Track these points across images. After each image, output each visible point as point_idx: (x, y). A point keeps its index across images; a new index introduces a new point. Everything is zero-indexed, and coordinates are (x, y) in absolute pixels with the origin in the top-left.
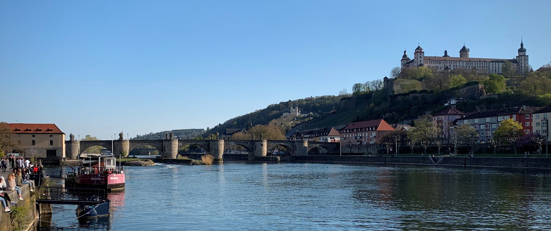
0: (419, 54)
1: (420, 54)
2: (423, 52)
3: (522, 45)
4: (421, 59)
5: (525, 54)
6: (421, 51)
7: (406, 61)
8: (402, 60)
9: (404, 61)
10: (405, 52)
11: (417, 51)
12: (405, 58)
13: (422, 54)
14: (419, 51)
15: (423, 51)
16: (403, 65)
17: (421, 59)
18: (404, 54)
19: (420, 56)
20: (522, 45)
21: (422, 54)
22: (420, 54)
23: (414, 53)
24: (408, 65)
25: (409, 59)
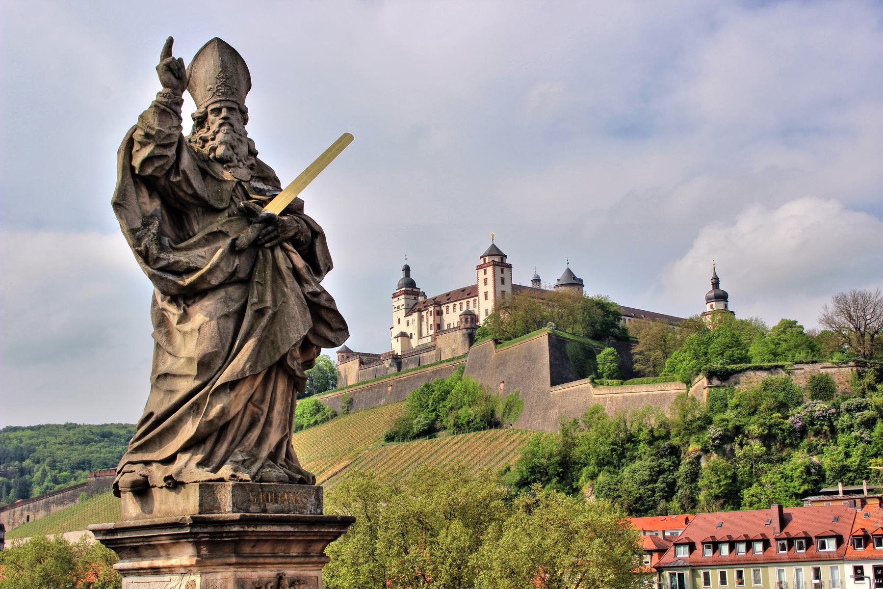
1: (502, 272)
2: (509, 266)
3: (716, 283)
4: (503, 288)
5: (726, 306)
6: (502, 259)
7: (413, 297)
9: (408, 296)
10: (407, 269)
12: (410, 289)
13: (505, 270)
14: (497, 259)
15: (508, 261)
17: (503, 288)
19: (503, 276)
20: (716, 283)
21: (505, 270)
22: (502, 272)
23: (479, 267)
24: (438, 309)
25: (424, 295)
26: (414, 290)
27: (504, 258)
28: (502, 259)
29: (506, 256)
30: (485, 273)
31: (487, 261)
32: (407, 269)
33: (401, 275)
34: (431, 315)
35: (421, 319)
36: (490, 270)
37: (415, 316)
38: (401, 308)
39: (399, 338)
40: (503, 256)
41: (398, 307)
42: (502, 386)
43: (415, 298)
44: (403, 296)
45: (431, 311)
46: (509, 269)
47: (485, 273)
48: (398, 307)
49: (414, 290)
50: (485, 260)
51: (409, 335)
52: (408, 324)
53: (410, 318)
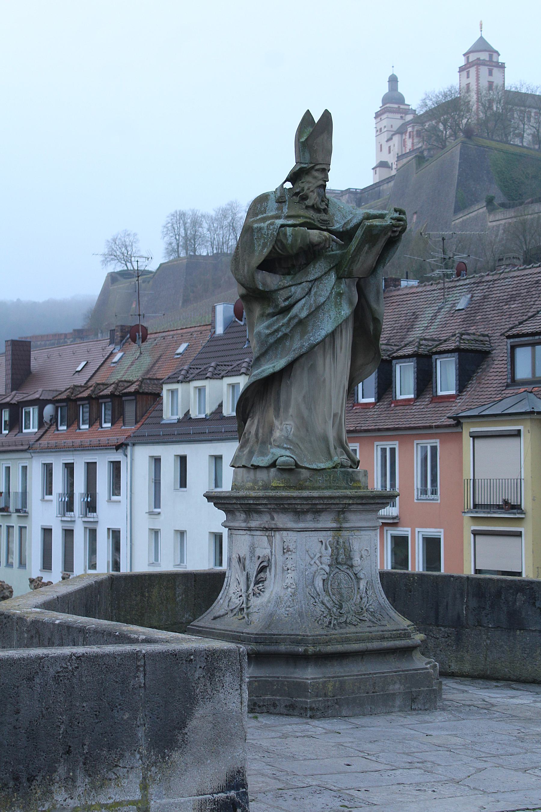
0: (484, 70)
1: (490, 73)
2: (502, 66)
6: (491, 56)
7: (398, 116)
8: (378, 115)
9: (391, 115)
10: (393, 80)
11: (473, 57)
13: (495, 71)
14: (484, 56)
15: (501, 60)
16: (385, 136)
18: (386, 90)
19: (491, 79)
21: (495, 71)
22: (490, 73)
23: (461, 69)
26: (402, 107)
27: (495, 55)
28: (491, 56)
29: (497, 52)
30: (468, 77)
31: (470, 60)
32: (393, 80)
33: (385, 89)
34: (410, 137)
35: (403, 143)
36: (473, 70)
37: (396, 139)
38: (383, 131)
39: (378, 169)
40: (492, 52)
41: (381, 129)
42: (415, 216)
43: (401, 117)
44: (385, 116)
45: (410, 132)
46: (501, 70)
47: (468, 77)
48: (381, 129)
49: (402, 107)
50: (468, 58)
51: (391, 165)
52: (390, 152)
53: (391, 143)
